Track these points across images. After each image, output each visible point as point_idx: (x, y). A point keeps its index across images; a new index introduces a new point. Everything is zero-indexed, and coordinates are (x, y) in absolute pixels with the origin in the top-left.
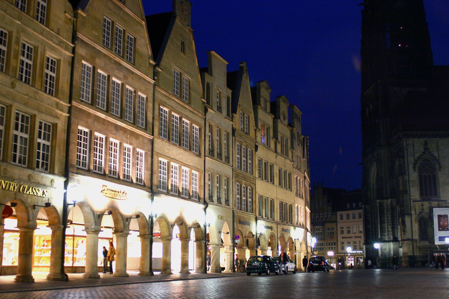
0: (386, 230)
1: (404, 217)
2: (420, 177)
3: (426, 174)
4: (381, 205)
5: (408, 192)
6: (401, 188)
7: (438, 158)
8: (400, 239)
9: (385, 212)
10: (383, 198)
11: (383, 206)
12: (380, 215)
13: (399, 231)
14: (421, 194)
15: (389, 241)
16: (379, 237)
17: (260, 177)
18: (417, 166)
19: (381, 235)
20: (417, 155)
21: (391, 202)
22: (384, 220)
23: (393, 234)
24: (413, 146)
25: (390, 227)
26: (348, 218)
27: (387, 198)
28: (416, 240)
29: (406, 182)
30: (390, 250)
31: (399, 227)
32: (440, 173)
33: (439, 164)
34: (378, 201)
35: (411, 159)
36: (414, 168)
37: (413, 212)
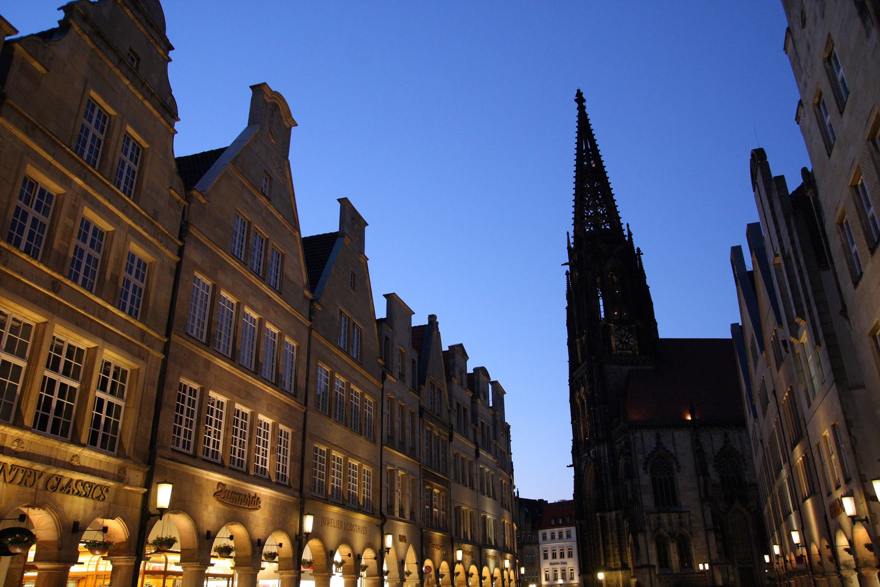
6: (630, 496)
8: (631, 566)
9: (609, 529)
12: (602, 533)
13: (629, 554)
14: (657, 504)
15: (616, 569)
16: (603, 563)
17: (456, 479)
19: (605, 561)
21: (617, 514)
23: (622, 559)
24: (642, 440)
25: (617, 549)
26: (561, 536)
27: (610, 511)
28: (654, 567)
31: (629, 550)
33: (677, 463)
34: (598, 514)
35: (640, 457)
36: (645, 468)
37: (647, 528)
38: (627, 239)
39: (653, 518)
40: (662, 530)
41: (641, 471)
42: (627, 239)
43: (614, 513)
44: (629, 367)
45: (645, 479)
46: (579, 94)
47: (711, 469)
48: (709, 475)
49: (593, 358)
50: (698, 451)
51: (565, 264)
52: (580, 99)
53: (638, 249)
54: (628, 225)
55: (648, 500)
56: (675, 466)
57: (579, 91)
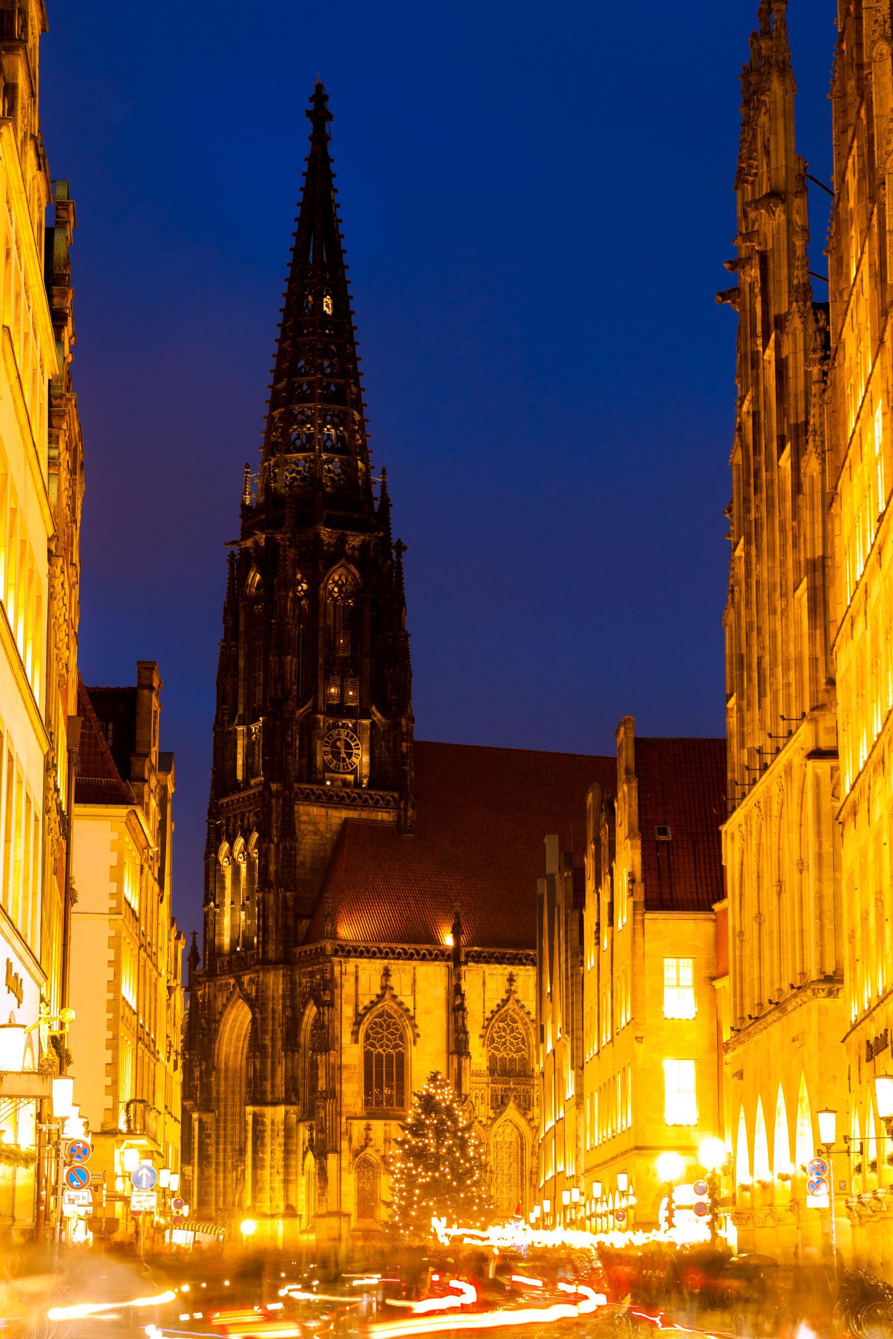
0: (267, 1186)
1: (326, 1158)
2: (368, 1056)
3: (381, 1050)
4: (258, 1120)
5: (338, 1095)
6: (322, 1084)
7: (412, 1013)
8: (302, 1210)
9: (268, 1140)
10: (265, 1103)
11: (263, 1124)
12: (254, 1144)
13: (302, 1189)
15: (272, 1216)
16: (248, 1202)
18: (363, 1028)
19: (254, 1199)
20: (365, 1001)
21: (287, 1113)
22: (263, 1159)
24: (357, 978)
27: (274, 1103)
29: (333, 1068)
30: (273, 1237)
31: (303, 1180)
32: (414, 1048)
33: (415, 1026)
34: (249, 1109)
35: (348, 1011)
36: (355, 1033)
37: (345, 1144)
38: (377, 504)
39: (358, 1127)
40: (369, 1150)
41: (347, 1038)
42: (377, 504)
43: (281, 1110)
44: (345, 814)
45: (352, 1054)
46: (320, 98)
47: (475, 1044)
48: (468, 1054)
49: (274, 787)
50: (456, 1007)
51: (233, 543)
52: (320, 115)
53: (399, 543)
54: (384, 472)
55: (352, 1092)
56: (409, 1034)
57: (319, 87)
